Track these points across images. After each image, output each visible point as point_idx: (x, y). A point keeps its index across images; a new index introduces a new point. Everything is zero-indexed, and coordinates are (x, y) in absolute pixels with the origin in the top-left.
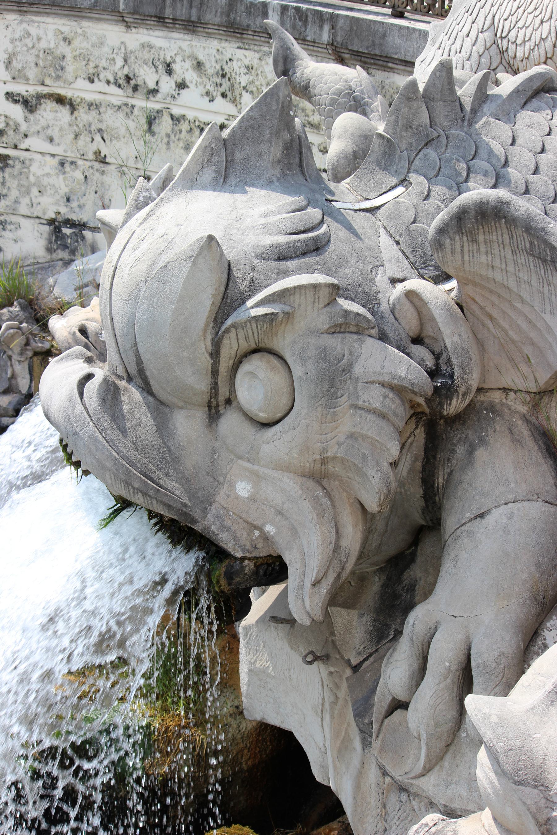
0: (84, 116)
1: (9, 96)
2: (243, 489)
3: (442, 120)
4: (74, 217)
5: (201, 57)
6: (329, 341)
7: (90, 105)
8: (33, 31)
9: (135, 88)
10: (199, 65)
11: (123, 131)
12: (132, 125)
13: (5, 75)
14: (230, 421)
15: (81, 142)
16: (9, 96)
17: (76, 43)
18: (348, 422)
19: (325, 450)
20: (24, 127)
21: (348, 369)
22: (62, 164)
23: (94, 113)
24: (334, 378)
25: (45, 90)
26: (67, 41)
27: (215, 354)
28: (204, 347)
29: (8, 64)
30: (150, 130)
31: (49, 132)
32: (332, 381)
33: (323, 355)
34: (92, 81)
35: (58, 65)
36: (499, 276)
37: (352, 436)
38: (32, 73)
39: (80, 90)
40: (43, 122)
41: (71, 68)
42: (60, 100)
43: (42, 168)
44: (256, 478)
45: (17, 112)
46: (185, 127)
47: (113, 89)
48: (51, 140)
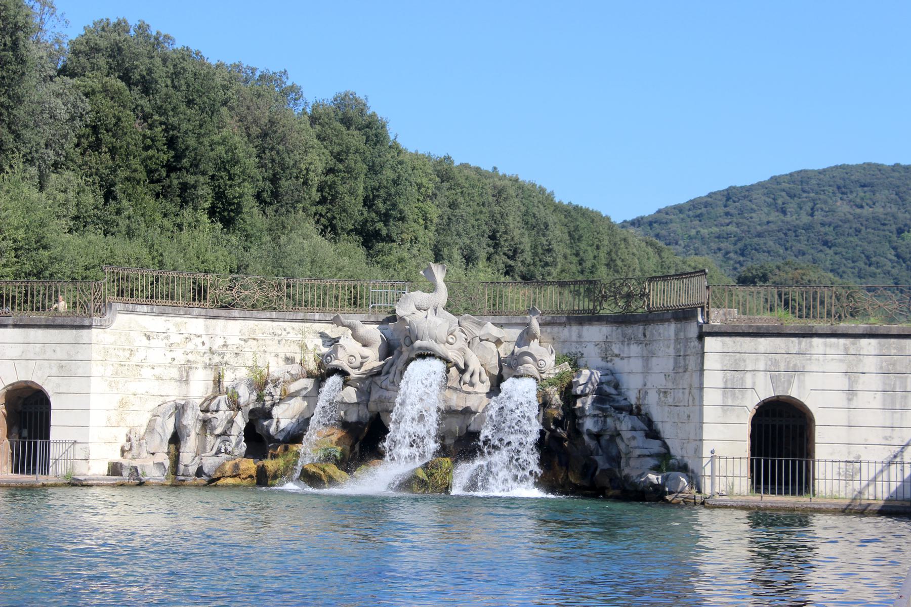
0: (260, 342)
39: (259, 336)
41: (257, 332)
45: (242, 343)
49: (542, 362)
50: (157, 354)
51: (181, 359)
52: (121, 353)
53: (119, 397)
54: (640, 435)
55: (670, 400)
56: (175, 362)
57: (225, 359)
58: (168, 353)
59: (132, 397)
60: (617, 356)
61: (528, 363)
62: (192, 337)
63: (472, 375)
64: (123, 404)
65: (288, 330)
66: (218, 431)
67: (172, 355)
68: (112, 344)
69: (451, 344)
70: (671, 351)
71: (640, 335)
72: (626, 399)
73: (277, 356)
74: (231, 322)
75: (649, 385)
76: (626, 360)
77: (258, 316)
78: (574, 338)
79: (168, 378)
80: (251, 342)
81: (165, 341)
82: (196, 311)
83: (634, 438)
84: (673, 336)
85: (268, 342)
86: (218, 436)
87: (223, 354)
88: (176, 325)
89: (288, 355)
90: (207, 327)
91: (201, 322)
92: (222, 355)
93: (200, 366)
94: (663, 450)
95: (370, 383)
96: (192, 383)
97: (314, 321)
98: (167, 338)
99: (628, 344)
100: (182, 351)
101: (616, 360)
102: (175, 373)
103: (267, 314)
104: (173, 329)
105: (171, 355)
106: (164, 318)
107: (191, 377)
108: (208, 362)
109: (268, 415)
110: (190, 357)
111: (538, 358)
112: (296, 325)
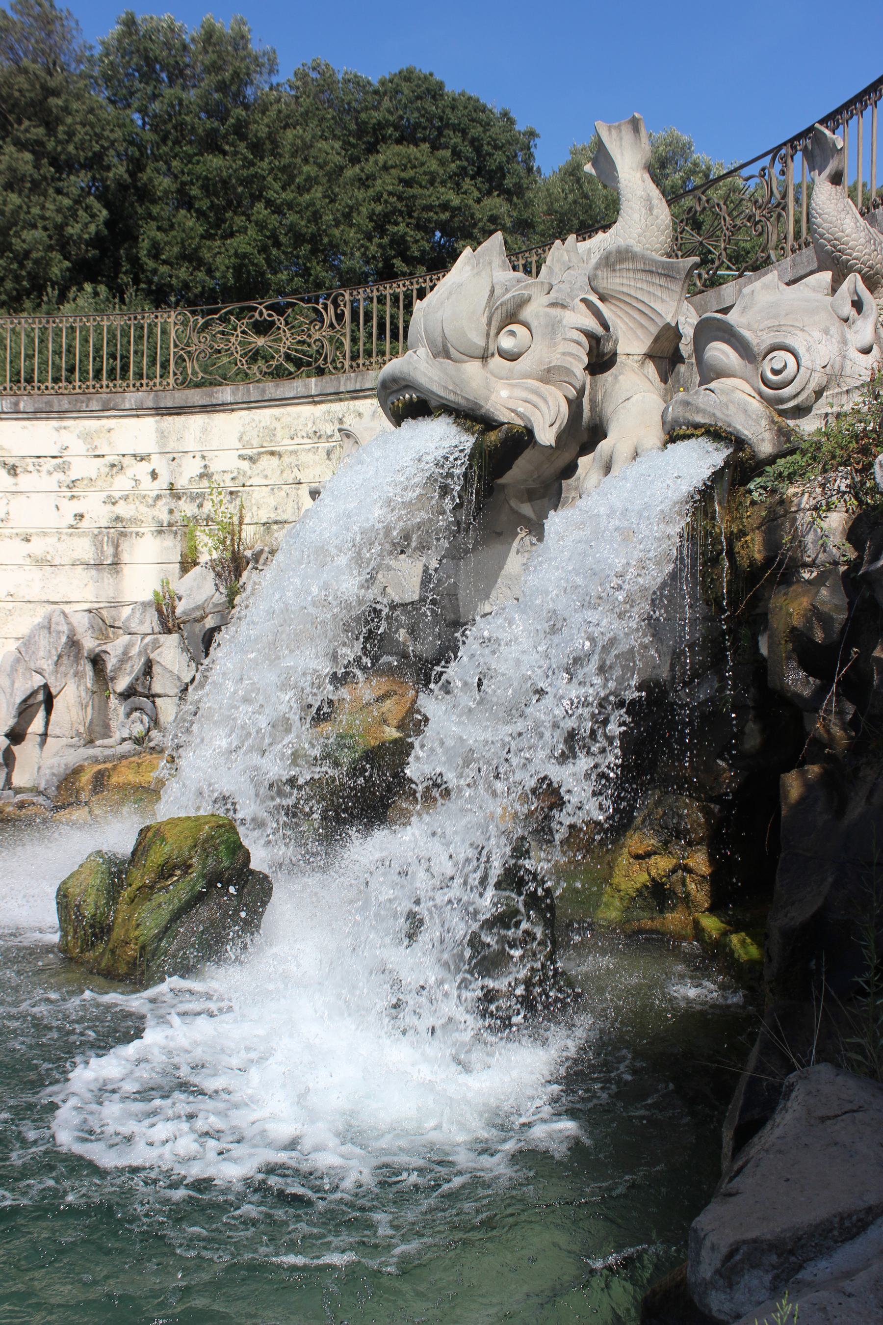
0: (286, 459)
1: (241, 457)
2: (504, 393)
3: (574, 260)
4: (279, 518)
5: (361, 410)
6: (549, 310)
7: (292, 452)
8: (256, 418)
9: (320, 437)
11: (311, 463)
12: (317, 457)
15: (285, 475)
16: (241, 457)
17: (283, 420)
18: (563, 347)
19: (550, 362)
20: (249, 473)
21: (560, 322)
22: (273, 489)
23: (293, 457)
24: (554, 326)
25: (263, 450)
26: (278, 419)
27: (489, 324)
28: (484, 320)
29: (240, 439)
30: (329, 458)
31: (265, 473)
32: (553, 326)
33: (547, 315)
34: (292, 439)
35: (273, 433)
36: (625, 290)
37: (564, 354)
38: (255, 443)
39: (284, 444)
40: (261, 468)
41: (279, 433)
42: (272, 453)
43: (259, 495)
45: (245, 465)
47: (306, 441)
48: (266, 477)
49: (781, 358)
56: (85, 523)
57: (208, 507)
58: (65, 504)
61: (720, 373)
62: (126, 461)
63: (607, 469)
66: (122, 684)
67: (77, 507)
69: (512, 357)
74: (220, 419)
77: (279, 394)
79: (66, 560)
80: (268, 463)
82: (131, 398)
85: (305, 458)
86: (127, 695)
87: (201, 495)
88: (86, 436)
90: (162, 436)
91: (149, 423)
92: (198, 498)
93: (147, 529)
96: (126, 570)
98: (63, 468)
102: (84, 549)
103: (296, 387)
104: (78, 447)
105: (71, 508)
106: (54, 423)
107: (125, 557)
108: (165, 517)
110: (122, 510)
111: (758, 339)
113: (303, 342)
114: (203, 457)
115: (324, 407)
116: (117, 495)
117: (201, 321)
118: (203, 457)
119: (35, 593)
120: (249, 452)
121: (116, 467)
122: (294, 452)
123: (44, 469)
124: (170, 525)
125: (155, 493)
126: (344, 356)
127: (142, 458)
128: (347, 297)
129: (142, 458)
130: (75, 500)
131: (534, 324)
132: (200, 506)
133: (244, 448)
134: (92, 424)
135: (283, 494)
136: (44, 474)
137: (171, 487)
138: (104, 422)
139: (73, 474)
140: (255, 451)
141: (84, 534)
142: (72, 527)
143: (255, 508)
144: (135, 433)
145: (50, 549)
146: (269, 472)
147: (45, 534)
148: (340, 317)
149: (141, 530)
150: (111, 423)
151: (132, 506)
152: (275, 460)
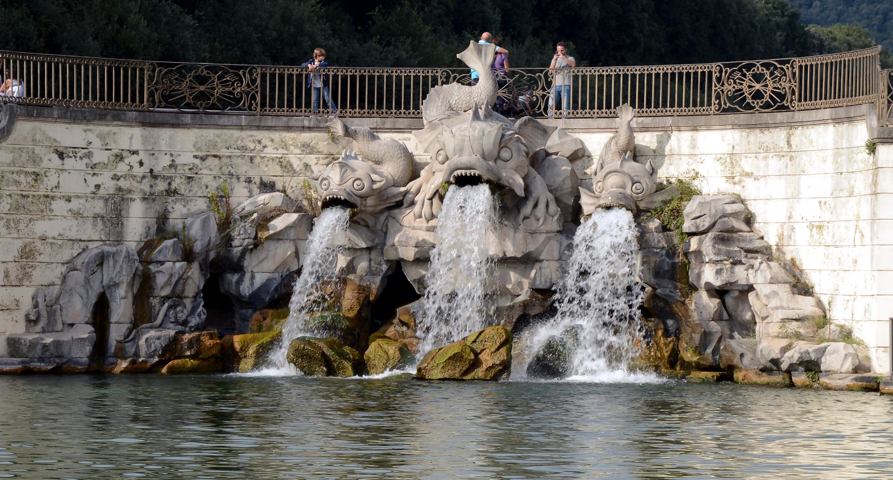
0: (224, 160)
1: (195, 157)
10: (272, 140)
13: (193, 150)
14: (499, 162)
16: (195, 157)
20: (200, 166)
24: (519, 150)
26: (218, 136)
30: (252, 162)
38: (204, 148)
39: (224, 152)
41: (219, 145)
42: (215, 156)
43: (207, 179)
44: (506, 172)
45: (197, 162)
46: (266, 159)
47: (237, 151)
50: (73, 179)
51: (109, 186)
52: (22, 178)
53: (19, 244)
54: (784, 290)
55: (827, 238)
56: (102, 192)
58: (89, 178)
59: (39, 244)
60: (748, 175)
62: (125, 154)
63: (536, 205)
64: (27, 254)
65: (264, 142)
68: (9, 165)
70: (829, 167)
71: (783, 143)
72: (762, 238)
73: (249, 181)
75: (796, 216)
76: (762, 180)
78: (685, 150)
80: (211, 161)
81: (86, 160)
83: (775, 293)
84: (831, 146)
88: (101, 136)
89: (266, 179)
90: (145, 139)
94: (819, 312)
95: (387, 219)
97: (303, 129)
98: (89, 155)
99: (765, 158)
100: (112, 174)
101: (748, 181)
102: (99, 207)
104: (97, 143)
106: (83, 127)
108: (147, 189)
109: (238, 268)
110: (122, 183)
112: (276, 135)
113: (230, 93)
114: (172, 155)
115: (249, 133)
116: (119, 174)
117: (165, 70)
118: (172, 155)
119: (73, 235)
120: (200, 154)
121: (120, 157)
122: (230, 157)
123: (78, 155)
124: (151, 194)
125: (141, 175)
126: (257, 105)
127: (135, 153)
128: (259, 70)
129: (135, 153)
130: (95, 177)
131: (514, 149)
132: (170, 184)
133: (197, 150)
134: (104, 129)
135: (222, 180)
136: (78, 159)
137: (151, 171)
138: (110, 128)
139: (95, 160)
140: (204, 154)
141: (101, 198)
142: (93, 193)
143: (204, 187)
144: (129, 136)
145: (82, 207)
146: (212, 167)
147: (78, 197)
148: (253, 81)
149: (134, 197)
150: (116, 129)
151: (128, 182)
152: (216, 160)
